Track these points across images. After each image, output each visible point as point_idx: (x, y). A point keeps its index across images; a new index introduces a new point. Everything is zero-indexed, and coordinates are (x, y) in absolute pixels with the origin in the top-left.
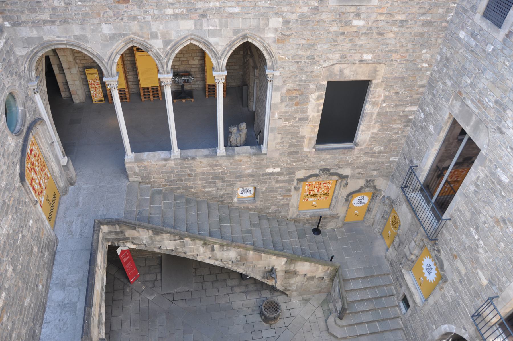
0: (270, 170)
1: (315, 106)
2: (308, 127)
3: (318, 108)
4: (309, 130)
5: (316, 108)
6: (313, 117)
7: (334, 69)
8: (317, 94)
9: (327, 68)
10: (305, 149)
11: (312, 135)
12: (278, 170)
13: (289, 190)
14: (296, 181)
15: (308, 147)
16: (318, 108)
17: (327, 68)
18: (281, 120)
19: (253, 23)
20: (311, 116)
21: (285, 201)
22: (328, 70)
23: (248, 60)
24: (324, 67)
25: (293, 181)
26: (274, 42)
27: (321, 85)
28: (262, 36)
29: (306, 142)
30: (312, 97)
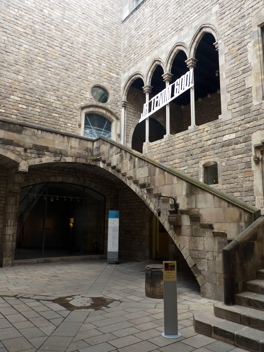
0: (227, 138)
1: (254, 53)
2: (252, 76)
3: (256, 53)
4: (254, 79)
5: (255, 55)
6: (254, 64)
7: (261, 13)
8: (252, 42)
9: (255, 16)
10: (255, 103)
11: (258, 85)
12: (233, 136)
13: (248, 165)
14: (253, 149)
15: (257, 100)
16: (256, 53)
17: (255, 16)
18: (228, 79)
19: (204, 17)
20: (252, 64)
21: (247, 185)
22: (257, 17)
23: (207, 45)
24: (253, 17)
25: (250, 150)
26: (217, 21)
27: (254, 32)
28: (209, 22)
29: (254, 94)
30: (249, 46)
